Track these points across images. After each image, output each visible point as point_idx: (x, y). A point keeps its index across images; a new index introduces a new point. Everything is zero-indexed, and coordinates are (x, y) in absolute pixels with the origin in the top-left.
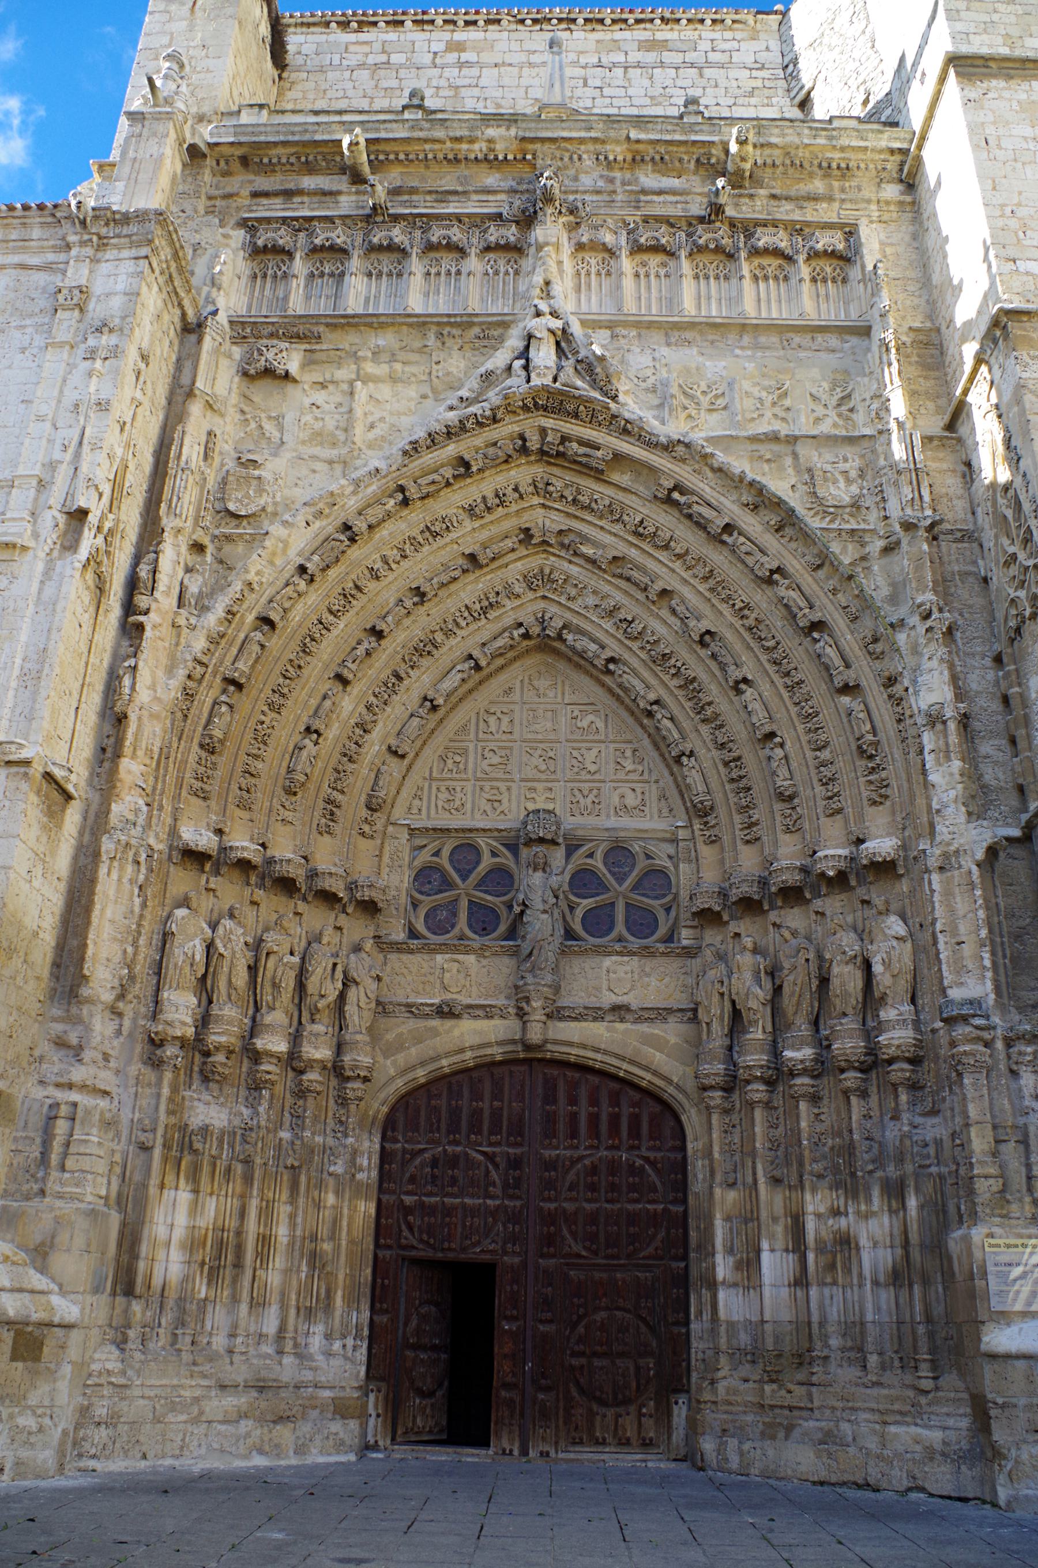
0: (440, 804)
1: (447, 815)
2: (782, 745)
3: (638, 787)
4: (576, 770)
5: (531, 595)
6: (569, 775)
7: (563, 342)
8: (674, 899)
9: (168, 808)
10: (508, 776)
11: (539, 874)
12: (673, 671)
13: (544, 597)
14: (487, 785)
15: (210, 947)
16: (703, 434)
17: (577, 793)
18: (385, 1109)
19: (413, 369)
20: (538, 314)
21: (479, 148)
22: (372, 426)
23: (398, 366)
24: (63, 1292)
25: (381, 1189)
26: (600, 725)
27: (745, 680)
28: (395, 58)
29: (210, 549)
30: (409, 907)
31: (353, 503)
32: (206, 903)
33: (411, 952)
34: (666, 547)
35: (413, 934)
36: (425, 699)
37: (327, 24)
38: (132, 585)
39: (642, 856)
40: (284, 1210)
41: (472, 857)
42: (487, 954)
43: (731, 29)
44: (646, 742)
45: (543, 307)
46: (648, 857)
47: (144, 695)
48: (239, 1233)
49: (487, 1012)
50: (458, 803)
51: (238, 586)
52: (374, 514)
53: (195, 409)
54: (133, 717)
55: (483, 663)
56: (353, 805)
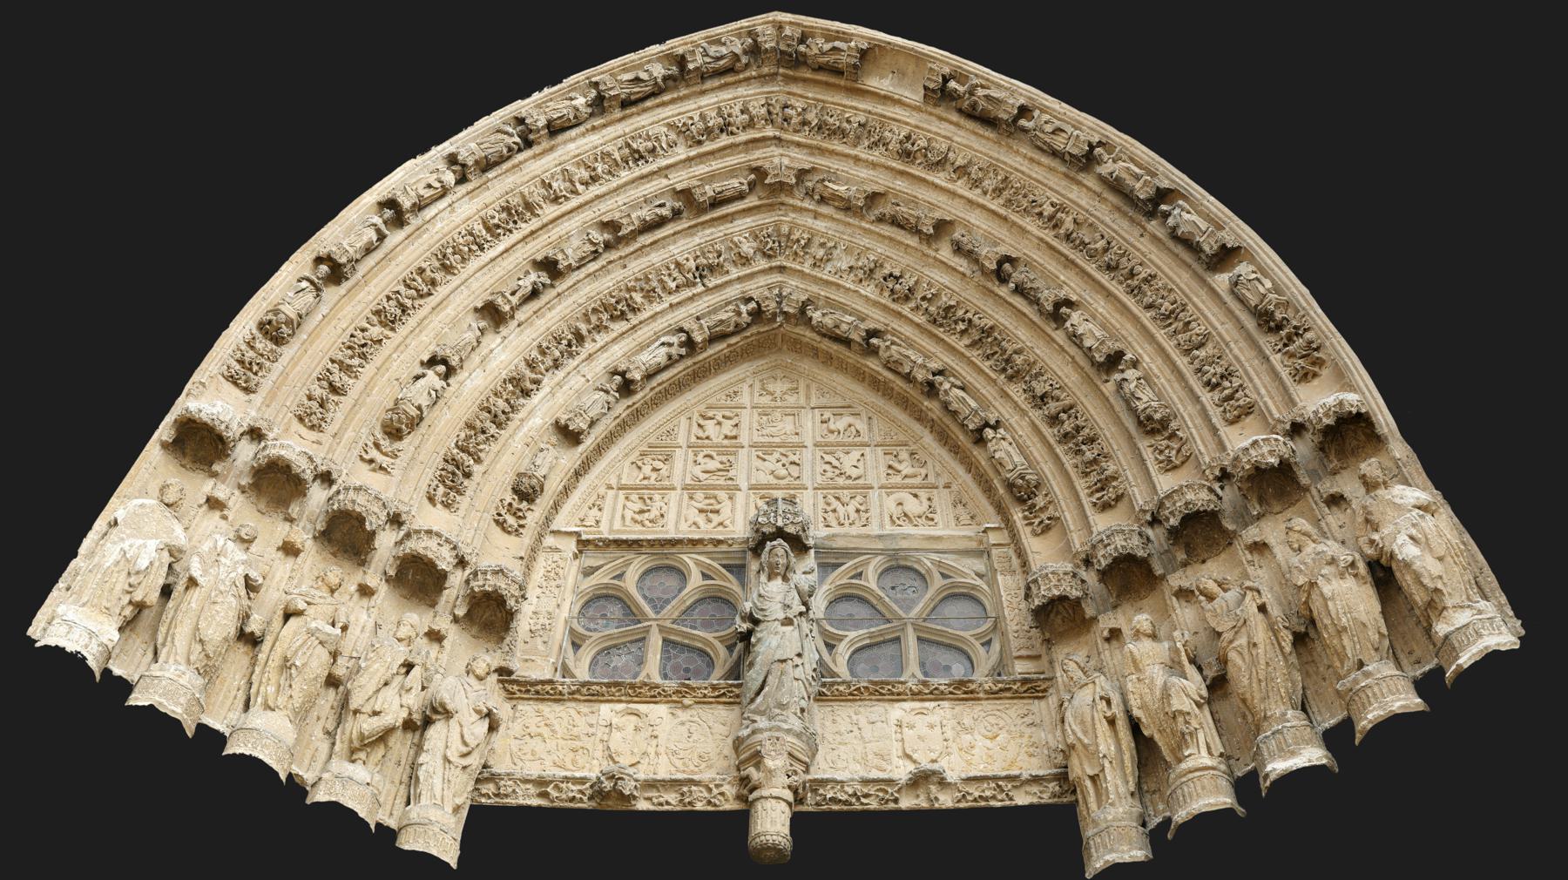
0: (629, 514)
1: (638, 527)
2: (1135, 364)
3: (923, 494)
4: (829, 474)
5: (763, 264)
6: (819, 479)
8: (995, 628)
10: (730, 482)
11: (778, 583)
12: (961, 326)
13: (782, 269)
14: (699, 495)
17: (833, 500)
26: (861, 425)
27: (1069, 303)
30: (567, 645)
33: (558, 698)
34: (940, 164)
39: (937, 576)
41: (671, 582)
42: (687, 701)
44: (928, 439)
50: (654, 513)
55: (698, 338)
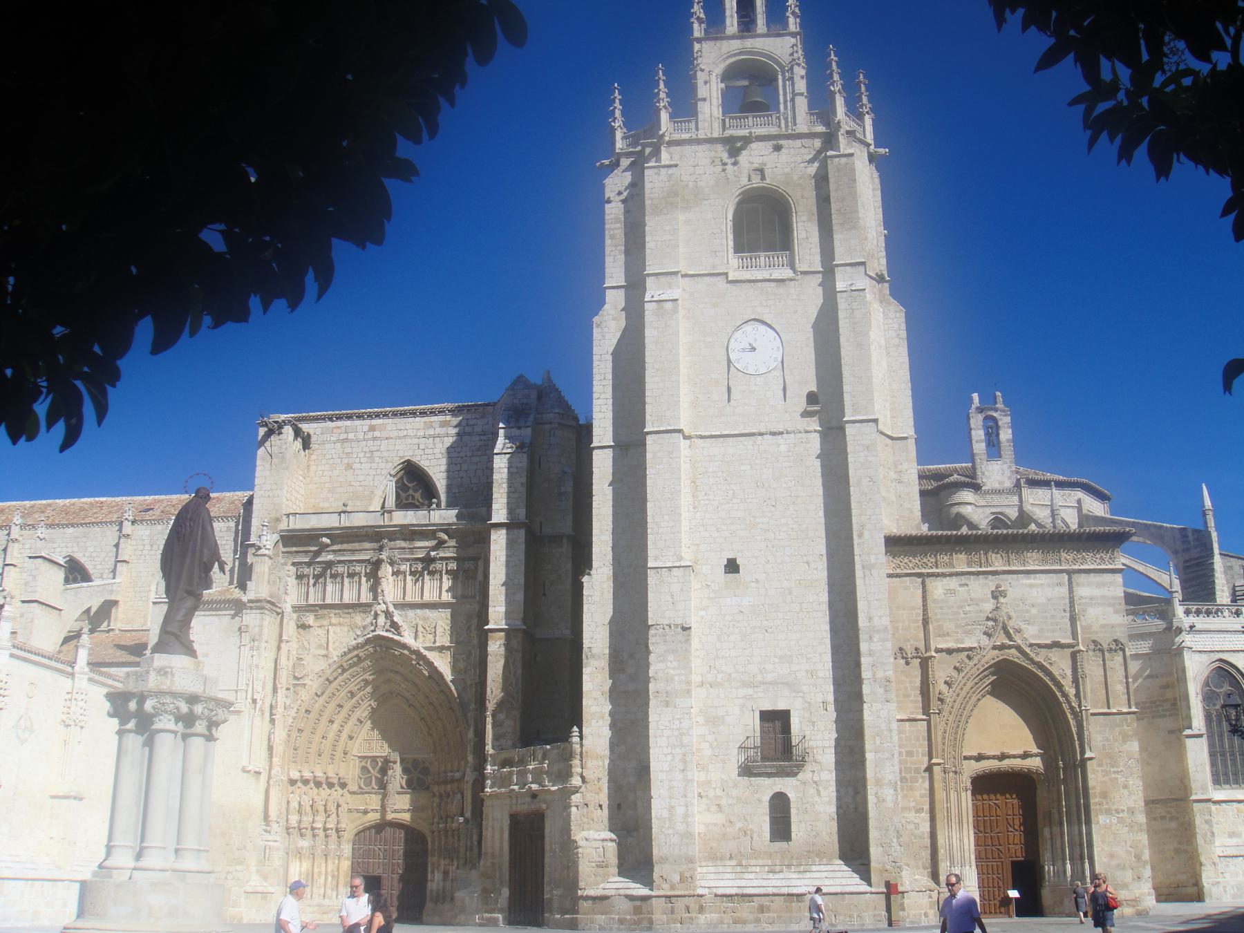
7: (388, 614)
9: (286, 767)
15: (300, 802)
16: (425, 645)
18: (352, 837)
19: (346, 620)
20: (379, 604)
21: (364, 533)
22: (334, 643)
23: (341, 620)
24: (271, 886)
25: (353, 858)
28: (351, 436)
29: (292, 688)
31: (329, 672)
32: (298, 790)
35: (360, 788)
36: (358, 719)
37: (324, 419)
38: (271, 707)
40: (324, 865)
43: (475, 412)
45: (381, 602)
46: (424, 763)
47: (277, 739)
48: (313, 871)
49: (376, 811)
51: (299, 701)
52: (335, 674)
53: (283, 645)
54: (274, 746)
56: (339, 754)
